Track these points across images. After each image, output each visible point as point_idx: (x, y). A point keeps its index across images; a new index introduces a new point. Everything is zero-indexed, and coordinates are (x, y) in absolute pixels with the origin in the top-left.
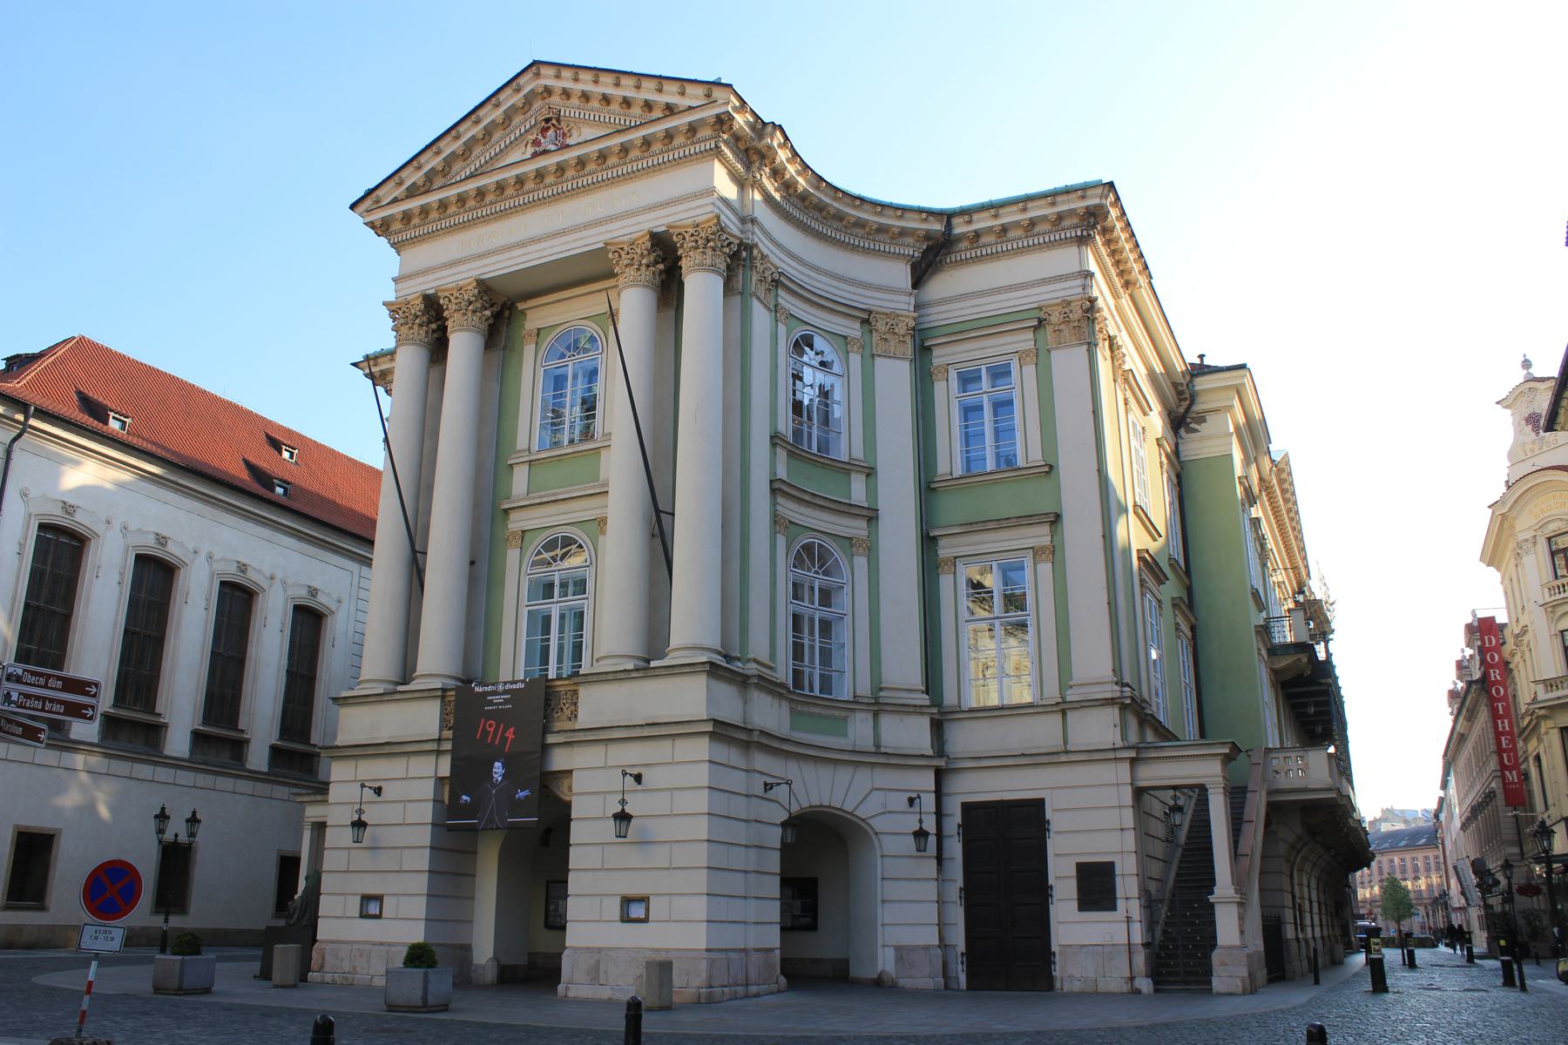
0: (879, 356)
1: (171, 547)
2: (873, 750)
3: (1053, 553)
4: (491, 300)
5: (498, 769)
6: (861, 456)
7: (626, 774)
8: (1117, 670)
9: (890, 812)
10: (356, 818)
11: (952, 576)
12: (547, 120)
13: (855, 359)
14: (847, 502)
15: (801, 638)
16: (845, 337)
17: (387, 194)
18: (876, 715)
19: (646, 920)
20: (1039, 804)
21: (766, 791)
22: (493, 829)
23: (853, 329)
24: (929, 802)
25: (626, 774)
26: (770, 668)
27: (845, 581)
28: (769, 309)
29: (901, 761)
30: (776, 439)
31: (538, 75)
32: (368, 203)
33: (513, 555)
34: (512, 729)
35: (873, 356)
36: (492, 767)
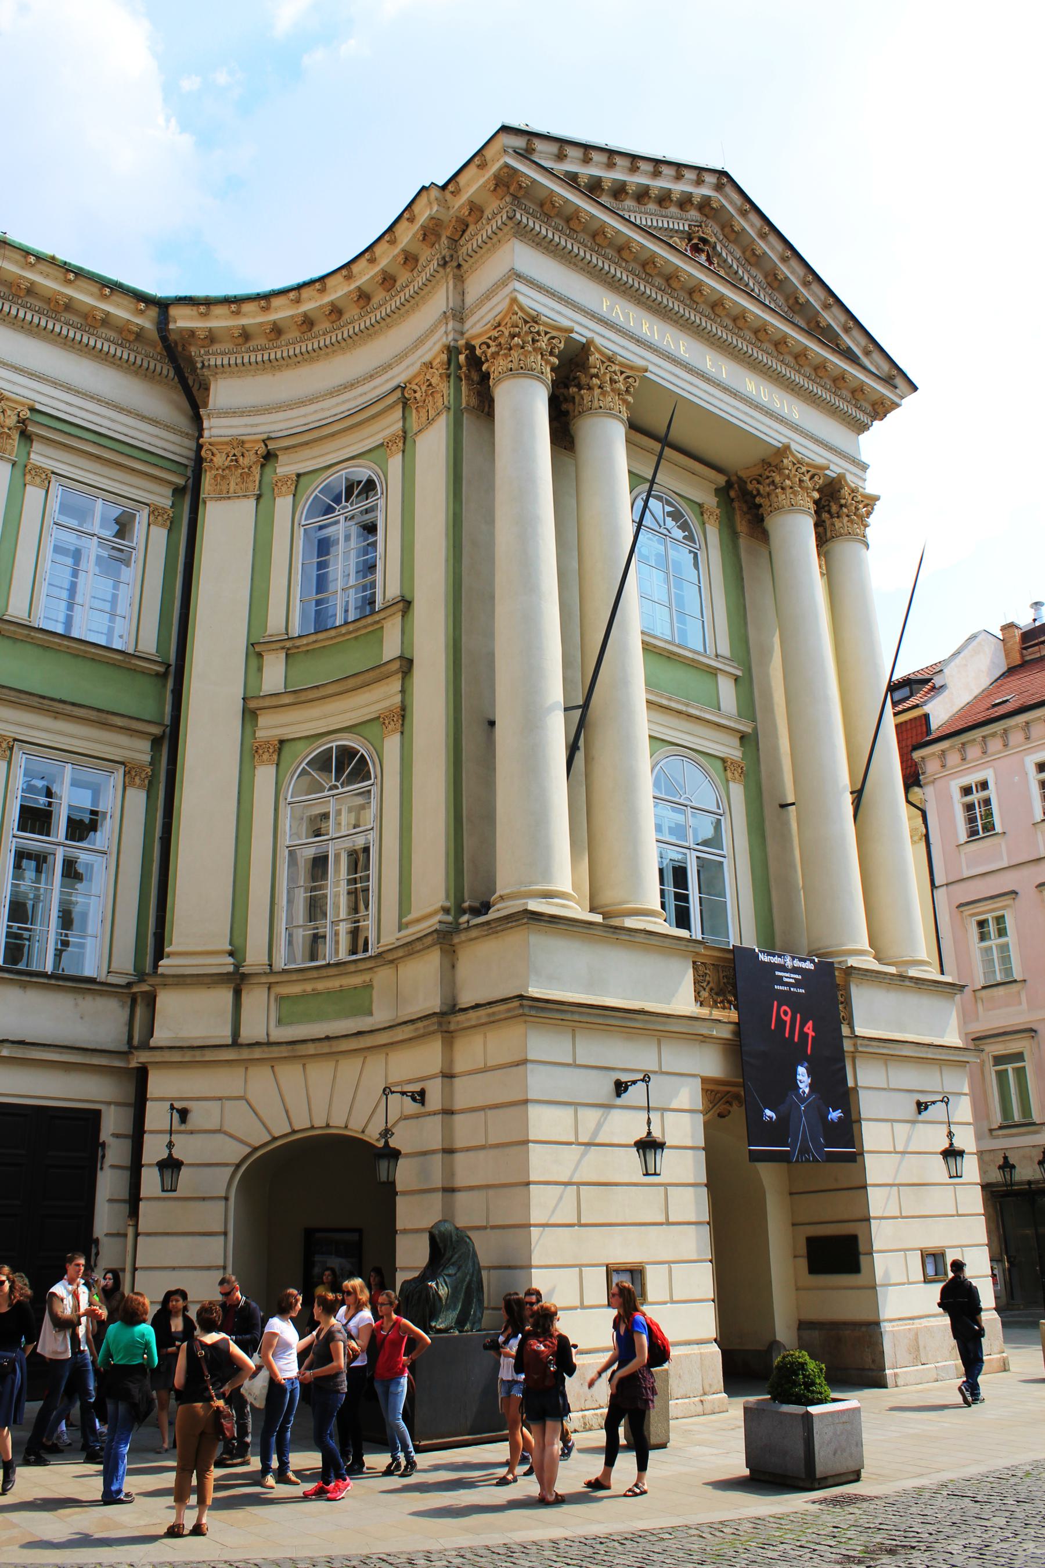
5: (803, 1076)
12: (704, 241)
22: (808, 1160)
32: (520, 142)
34: (810, 1024)
36: (795, 1073)
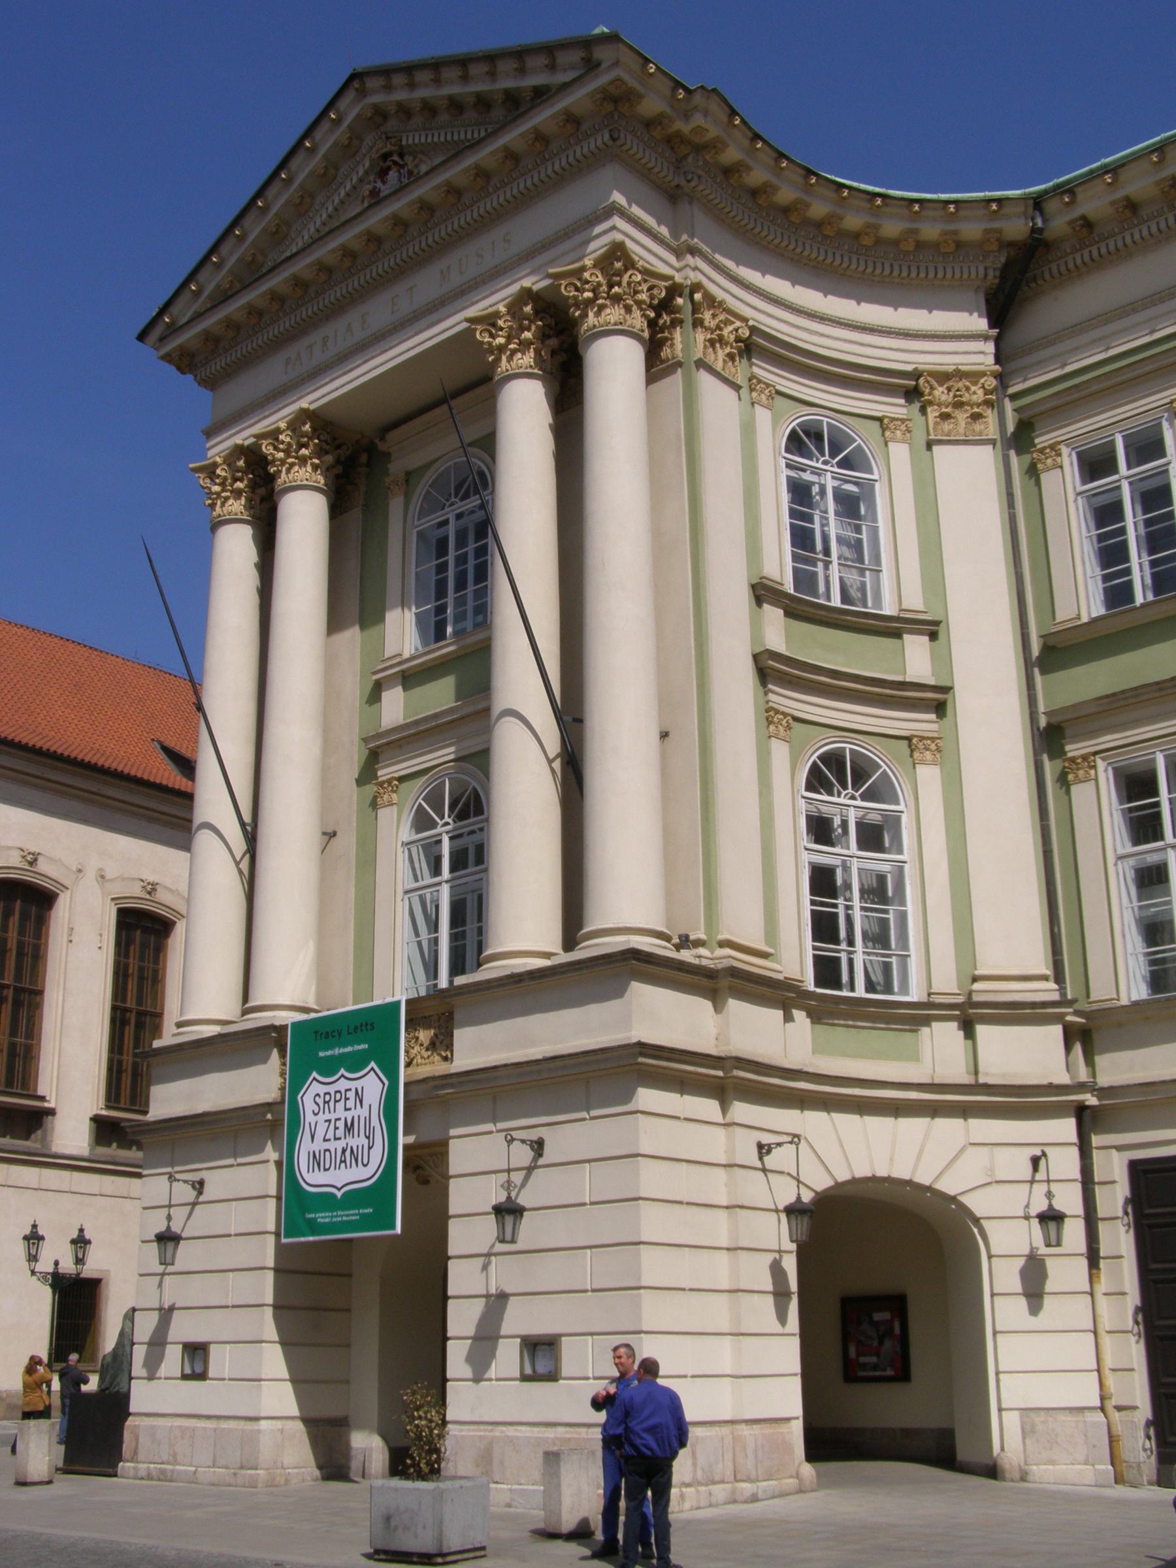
0: (940, 442)
1: (43, 866)
2: (967, 1079)
4: (335, 439)
7: (513, 1139)
9: (997, 1182)
10: (161, 1227)
11: (1093, 782)
12: (386, 156)
13: (899, 453)
15: (835, 906)
16: (880, 420)
17: (183, 311)
21: (761, 1158)
23: (894, 407)
24: (1065, 1162)
25: (513, 1139)
26: (764, 955)
27: (901, 807)
28: (737, 388)
31: (362, 93)
35: (929, 446)
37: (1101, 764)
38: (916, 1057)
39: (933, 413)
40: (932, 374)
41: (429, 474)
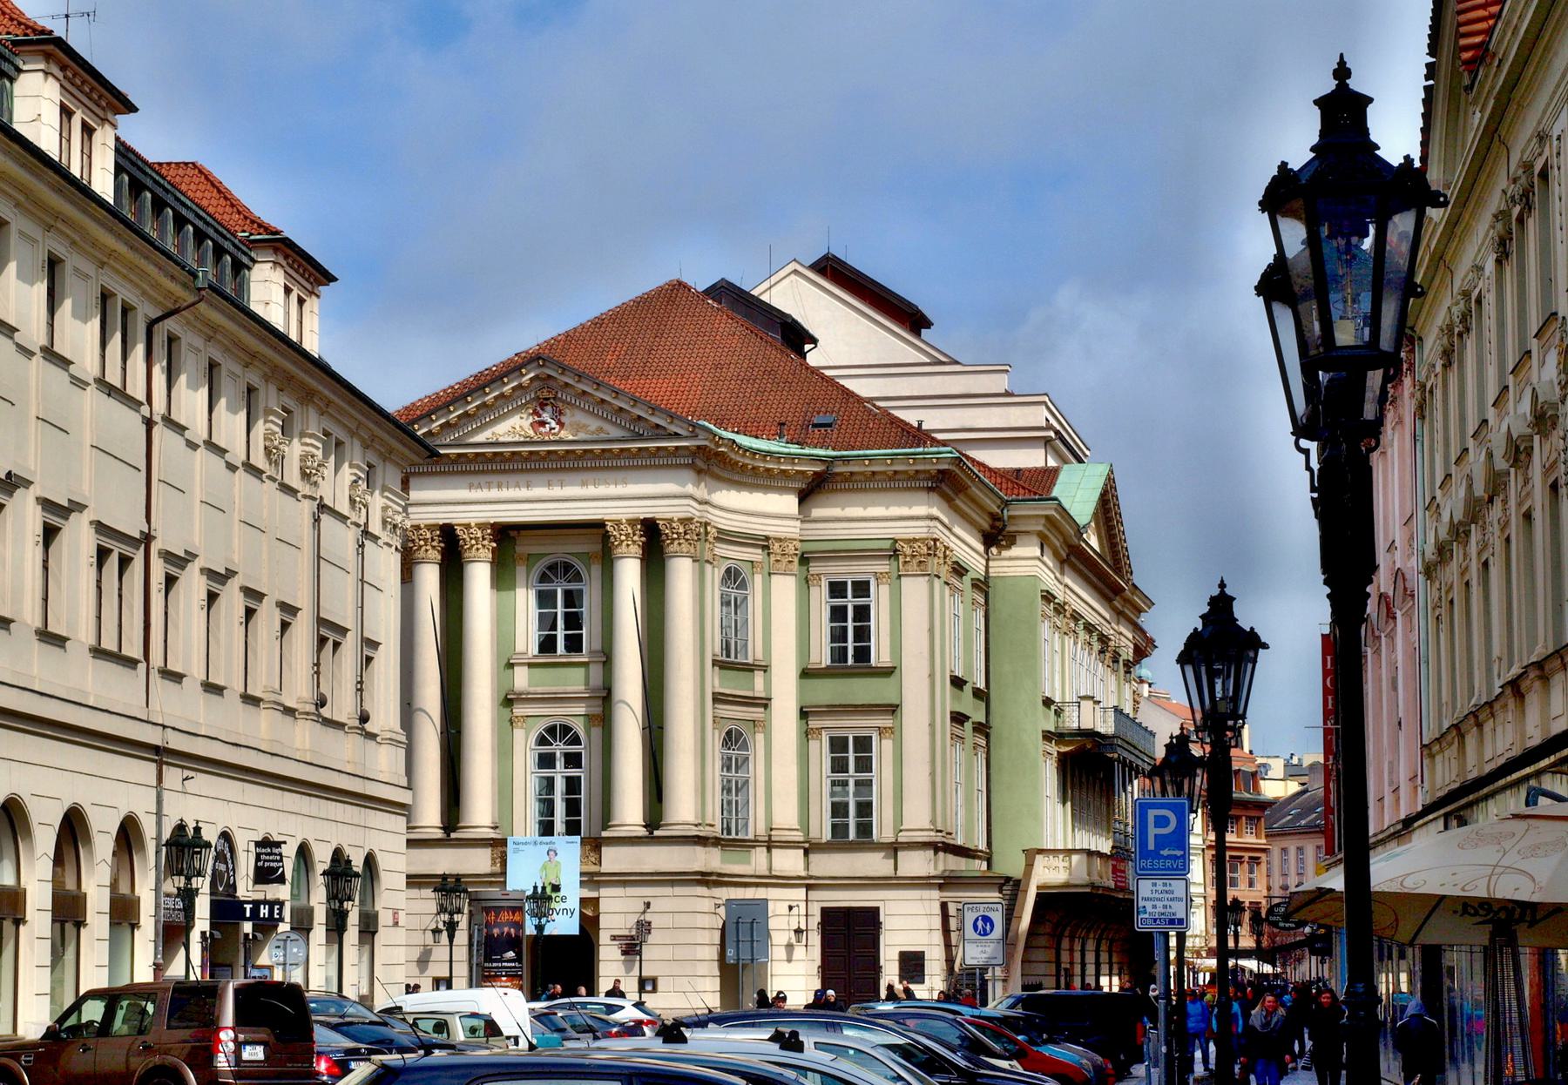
2: (767, 873)
3: (894, 732)
6: (761, 658)
8: (933, 822)
13: (758, 579)
14: (749, 694)
16: (752, 562)
18: (769, 849)
19: (654, 990)
20: (875, 912)
23: (756, 555)
29: (785, 882)
30: (715, 663)
33: (519, 734)
35: (770, 574)
37: (824, 733)
38: (749, 863)
39: (773, 558)
40: (775, 539)
41: (544, 560)
